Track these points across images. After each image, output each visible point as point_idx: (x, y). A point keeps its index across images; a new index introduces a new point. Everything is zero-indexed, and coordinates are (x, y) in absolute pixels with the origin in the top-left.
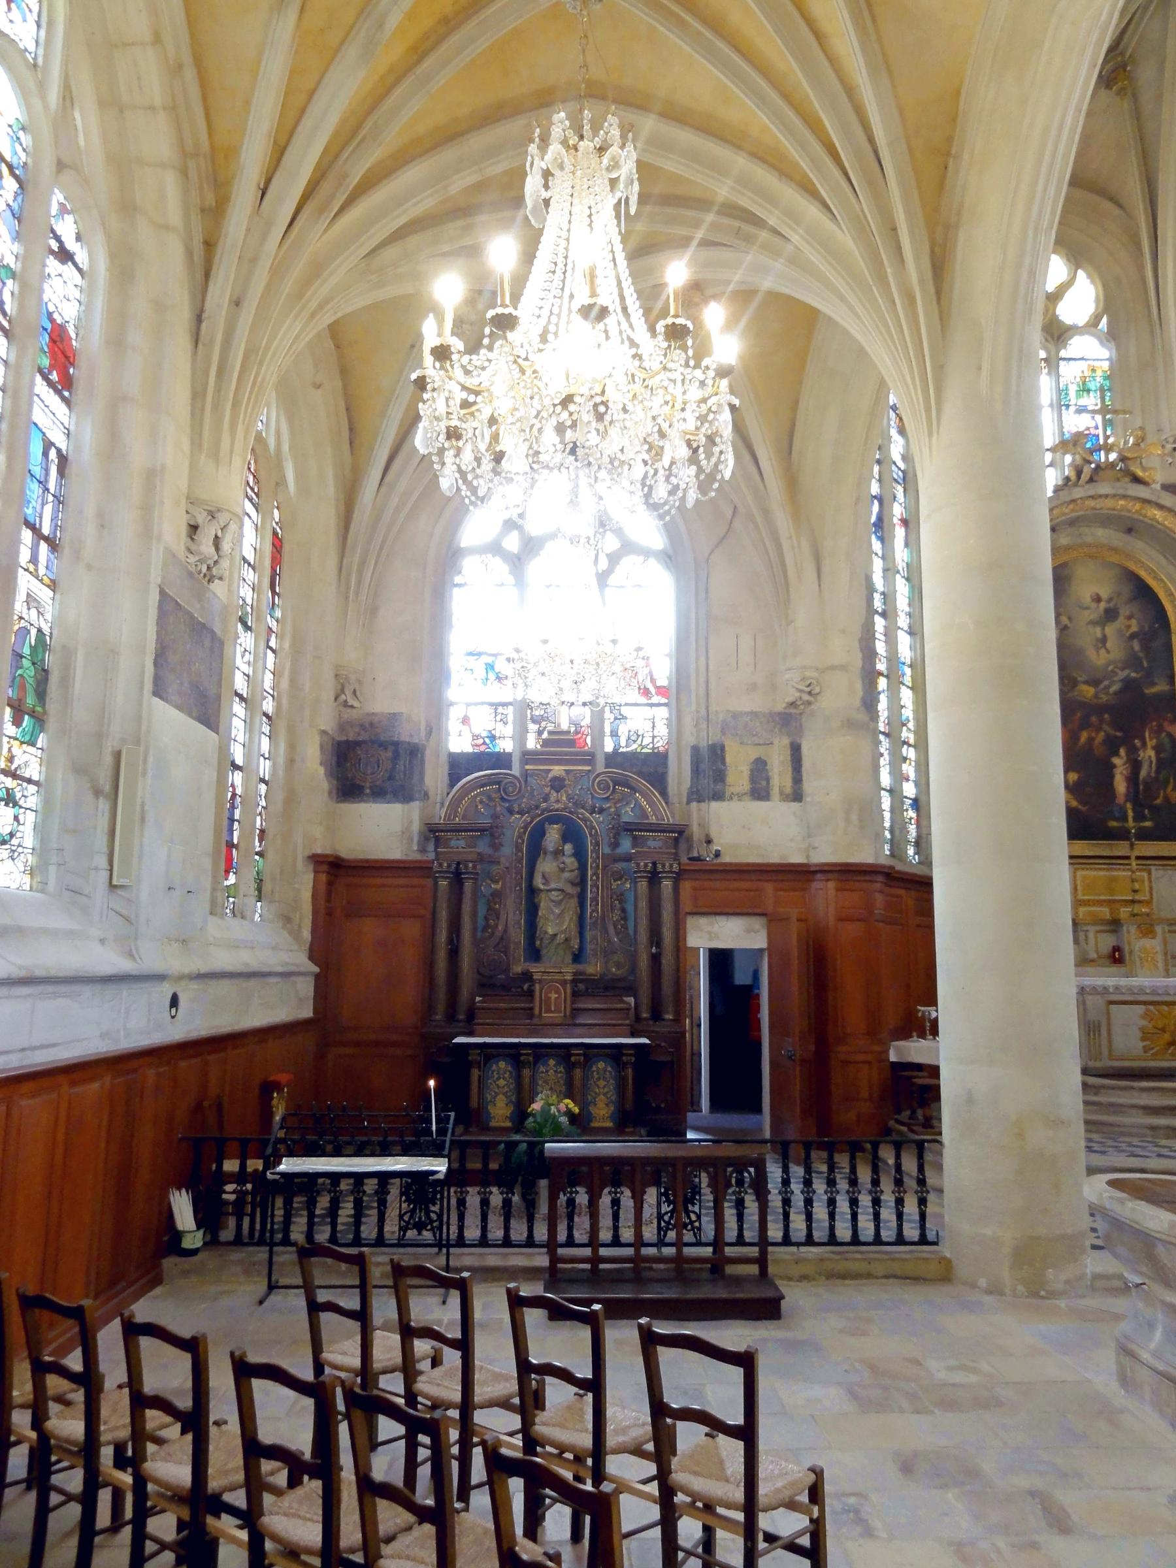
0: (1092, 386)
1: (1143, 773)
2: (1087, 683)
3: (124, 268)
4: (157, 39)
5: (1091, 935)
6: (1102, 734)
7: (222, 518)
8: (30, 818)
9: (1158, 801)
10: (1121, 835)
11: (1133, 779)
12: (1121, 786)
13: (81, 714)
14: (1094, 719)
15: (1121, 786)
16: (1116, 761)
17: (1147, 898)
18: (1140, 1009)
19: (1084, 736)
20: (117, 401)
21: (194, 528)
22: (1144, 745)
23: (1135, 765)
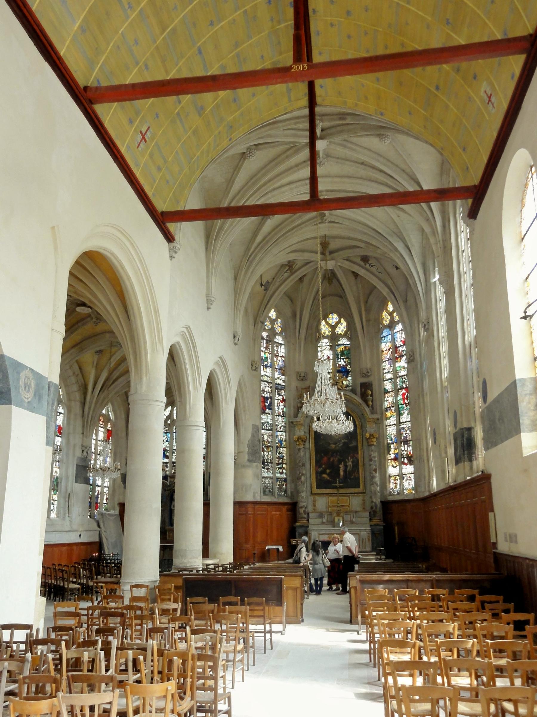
0: (345, 352)
1: (348, 469)
2: (333, 444)
3: (69, 410)
4: (74, 373)
5: (326, 516)
6: (337, 458)
7: (88, 448)
8: (56, 506)
9: (352, 477)
10: (335, 487)
11: (345, 471)
12: (342, 473)
13: (63, 488)
14: (335, 454)
15: (342, 473)
16: (341, 466)
17: (348, 504)
18: (327, 536)
19: (332, 459)
20: (69, 434)
21: (83, 451)
22: (348, 460)
23: (346, 467)
